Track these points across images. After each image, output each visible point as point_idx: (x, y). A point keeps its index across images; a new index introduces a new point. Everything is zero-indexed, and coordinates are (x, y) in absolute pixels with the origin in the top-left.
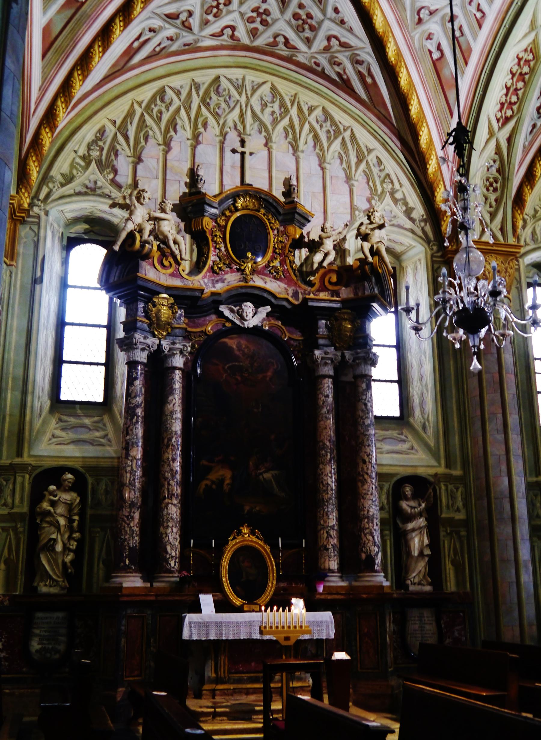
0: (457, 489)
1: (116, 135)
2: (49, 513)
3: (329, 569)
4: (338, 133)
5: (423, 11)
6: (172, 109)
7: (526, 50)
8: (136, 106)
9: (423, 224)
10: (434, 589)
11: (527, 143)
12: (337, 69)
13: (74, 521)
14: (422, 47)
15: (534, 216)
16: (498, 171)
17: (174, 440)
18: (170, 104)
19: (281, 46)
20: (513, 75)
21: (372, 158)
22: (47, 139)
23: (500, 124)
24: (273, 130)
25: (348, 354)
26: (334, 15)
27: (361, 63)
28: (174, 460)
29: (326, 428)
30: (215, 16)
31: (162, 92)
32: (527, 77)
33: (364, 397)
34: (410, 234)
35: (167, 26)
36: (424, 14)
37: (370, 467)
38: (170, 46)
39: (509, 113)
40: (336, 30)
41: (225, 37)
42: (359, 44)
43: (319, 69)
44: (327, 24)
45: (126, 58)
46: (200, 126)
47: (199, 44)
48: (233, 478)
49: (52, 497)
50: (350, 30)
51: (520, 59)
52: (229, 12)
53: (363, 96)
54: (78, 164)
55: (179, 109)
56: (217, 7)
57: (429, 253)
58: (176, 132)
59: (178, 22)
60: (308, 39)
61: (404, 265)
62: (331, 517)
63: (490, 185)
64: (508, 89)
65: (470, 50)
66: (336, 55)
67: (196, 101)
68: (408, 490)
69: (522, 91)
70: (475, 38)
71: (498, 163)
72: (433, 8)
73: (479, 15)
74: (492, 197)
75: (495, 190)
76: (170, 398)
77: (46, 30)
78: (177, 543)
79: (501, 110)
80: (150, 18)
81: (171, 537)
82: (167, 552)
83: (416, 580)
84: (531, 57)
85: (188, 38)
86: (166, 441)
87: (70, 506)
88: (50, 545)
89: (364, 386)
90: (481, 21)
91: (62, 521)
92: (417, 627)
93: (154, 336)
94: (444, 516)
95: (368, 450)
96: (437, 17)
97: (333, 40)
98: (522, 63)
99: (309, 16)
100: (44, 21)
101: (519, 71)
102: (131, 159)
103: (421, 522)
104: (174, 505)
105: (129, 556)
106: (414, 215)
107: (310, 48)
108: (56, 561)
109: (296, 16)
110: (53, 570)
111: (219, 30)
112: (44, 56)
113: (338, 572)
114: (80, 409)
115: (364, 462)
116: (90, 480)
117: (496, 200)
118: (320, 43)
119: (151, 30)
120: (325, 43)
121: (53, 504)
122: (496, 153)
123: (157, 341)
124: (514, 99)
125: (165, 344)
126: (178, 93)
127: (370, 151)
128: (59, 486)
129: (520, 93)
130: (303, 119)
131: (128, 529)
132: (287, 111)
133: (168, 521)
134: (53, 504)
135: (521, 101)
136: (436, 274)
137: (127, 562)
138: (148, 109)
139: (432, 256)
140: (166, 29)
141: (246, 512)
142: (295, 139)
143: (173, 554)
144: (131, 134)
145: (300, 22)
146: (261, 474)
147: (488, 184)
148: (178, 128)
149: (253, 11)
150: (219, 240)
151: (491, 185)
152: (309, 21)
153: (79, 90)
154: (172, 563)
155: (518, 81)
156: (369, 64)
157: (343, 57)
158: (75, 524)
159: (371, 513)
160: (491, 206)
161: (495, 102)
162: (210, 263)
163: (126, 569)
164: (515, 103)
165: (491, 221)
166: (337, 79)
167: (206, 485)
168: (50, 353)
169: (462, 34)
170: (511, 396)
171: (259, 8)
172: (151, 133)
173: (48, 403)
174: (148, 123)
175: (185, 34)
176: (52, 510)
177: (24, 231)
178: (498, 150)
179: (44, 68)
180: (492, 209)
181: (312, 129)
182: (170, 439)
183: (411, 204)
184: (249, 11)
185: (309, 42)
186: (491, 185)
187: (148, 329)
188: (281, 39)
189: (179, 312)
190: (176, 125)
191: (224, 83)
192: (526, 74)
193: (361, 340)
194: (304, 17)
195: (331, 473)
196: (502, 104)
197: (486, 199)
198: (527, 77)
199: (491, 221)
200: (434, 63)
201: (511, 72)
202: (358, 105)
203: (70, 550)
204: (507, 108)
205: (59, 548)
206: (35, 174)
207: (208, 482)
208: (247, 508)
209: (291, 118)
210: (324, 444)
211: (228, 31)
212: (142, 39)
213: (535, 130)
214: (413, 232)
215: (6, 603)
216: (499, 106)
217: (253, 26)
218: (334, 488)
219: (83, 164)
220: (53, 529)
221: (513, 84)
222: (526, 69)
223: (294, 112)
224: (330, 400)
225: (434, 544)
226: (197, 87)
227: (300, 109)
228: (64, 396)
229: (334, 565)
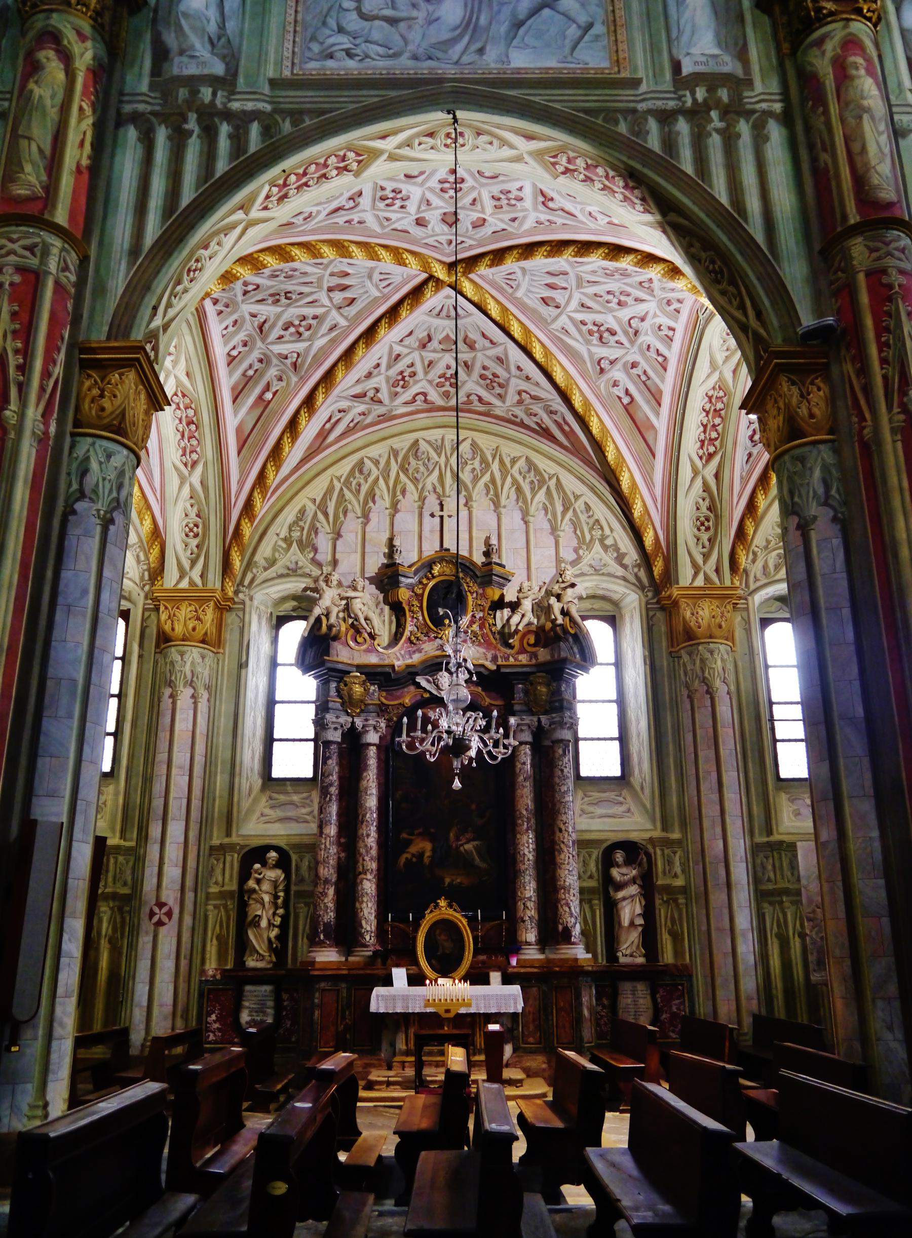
0: (675, 853)
1: (316, 512)
2: (254, 891)
3: (526, 942)
4: (542, 482)
5: (602, 361)
6: (370, 480)
7: (714, 388)
8: (336, 482)
9: (636, 570)
10: (647, 961)
11: (744, 474)
12: (535, 419)
13: (278, 897)
14: (610, 394)
15: (766, 547)
16: (709, 509)
17: (368, 815)
18: (369, 475)
19: (476, 403)
20: (707, 413)
21: (579, 505)
22: (247, 530)
23: (704, 462)
24: (474, 488)
25: (544, 719)
26: (518, 373)
27: (555, 413)
28: (368, 836)
29: (522, 797)
30: (403, 387)
31: (360, 465)
32: (723, 412)
33: (561, 763)
34: (622, 582)
35: (356, 404)
36: (604, 364)
37: (566, 835)
38: (364, 420)
39: (712, 449)
40: (524, 386)
41: (418, 403)
42: (551, 397)
43: (518, 420)
44: (513, 381)
45: (321, 439)
46: (398, 493)
47: (394, 413)
48: (434, 850)
49: (257, 876)
50: (537, 384)
51: (710, 398)
52: (416, 382)
53: (566, 443)
54: (280, 546)
55: (377, 479)
56: (403, 379)
57: (644, 600)
58: (374, 502)
59: (367, 399)
60: (499, 394)
61: (623, 612)
62: (527, 888)
63: (701, 524)
64: (705, 426)
65: (661, 392)
66: (530, 407)
67: (394, 468)
68: (619, 856)
69: (721, 426)
70: (663, 381)
71: (708, 500)
72: (612, 358)
73: (660, 359)
74: (705, 537)
75: (708, 529)
76: (365, 774)
77: (239, 430)
78: (372, 917)
79: (702, 447)
80: (336, 402)
81: (366, 911)
82: (362, 927)
83: (628, 952)
84: (721, 394)
85: (381, 410)
86: (360, 817)
87: (275, 884)
88: (256, 922)
89: (560, 751)
90: (664, 364)
91: (267, 898)
92: (629, 1001)
93: (348, 714)
94: (659, 882)
95: (564, 818)
96: (619, 366)
97: (524, 394)
98: (713, 400)
99: (495, 375)
100: (236, 422)
101: (713, 408)
102: (330, 536)
103: (633, 890)
104: (369, 880)
105: (324, 931)
106: (627, 561)
107: (504, 402)
108: (261, 936)
109: (482, 377)
110: (260, 945)
111: (411, 398)
112: (239, 453)
113: (537, 945)
114: (291, 785)
115: (561, 830)
116: (294, 857)
117: (709, 540)
118: (512, 398)
119: (340, 411)
120: (517, 397)
121: (258, 881)
122: (704, 491)
123: (350, 719)
124: (714, 435)
125: (359, 722)
126: (376, 463)
127: (577, 497)
128: (264, 864)
129: (720, 428)
130: (504, 472)
131: (322, 905)
132: (488, 466)
133: (362, 896)
134: (258, 881)
135: (722, 436)
136: (651, 623)
137: (322, 937)
138: (347, 483)
139: (647, 603)
140: (355, 407)
141: (446, 884)
142: (497, 495)
143: (369, 928)
144: (331, 511)
145: (488, 381)
146: (462, 845)
147: (699, 523)
148: (377, 498)
149: (440, 377)
150: (416, 609)
152: (496, 379)
153: (273, 479)
154: (368, 938)
155: (714, 417)
156: (562, 413)
157: (537, 408)
158: (280, 901)
159: (567, 884)
160: (703, 547)
161: (694, 441)
162: (407, 633)
163: (321, 944)
164: (716, 439)
165: (705, 562)
166: (537, 428)
167: (407, 858)
168: (260, 732)
169: (649, 378)
170: (727, 751)
171: (445, 374)
172: (350, 507)
173: (260, 782)
174: (347, 498)
175: (376, 407)
176: (257, 888)
177: (231, 619)
178: (706, 488)
179: (240, 464)
180: (705, 550)
181: (515, 482)
182: (364, 816)
183: (623, 550)
184: (436, 378)
185: (500, 396)
186: (702, 524)
187: (341, 708)
188: (474, 398)
189: (372, 688)
190: (375, 495)
191: (423, 446)
192: (721, 410)
193: (557, 704)
194: (491, 377)
195: (528, 842)
196: (702, 442)
197: (698, 540)
198: (723, 412)
199: (705, 562)
200: (626, 408)
201: (704, 410)
202: (563, 451)
203: (274, 926)
204: (708, 445)
205: (264, 923)
206: (237, 563)
207: (409, 856)
208: (447, 880)
209: (492, 474)
210: (521, 813)
211: (421, 397)
212: (333, 421)
213: (751, 459)
214: (624, 579)
215: (218, 977)
216: (699, 444)
217: (444, 389)
218: (531, 858)
219: (284, 546)
220: (259, 906)
221: (708, 420)
222: (719, 406)
223: (495, 467)
224: (528, 767)
225: (649, 913)
226: (395, 453)
227: (502, 462)
228: (275, 774)
229: (531, 936)
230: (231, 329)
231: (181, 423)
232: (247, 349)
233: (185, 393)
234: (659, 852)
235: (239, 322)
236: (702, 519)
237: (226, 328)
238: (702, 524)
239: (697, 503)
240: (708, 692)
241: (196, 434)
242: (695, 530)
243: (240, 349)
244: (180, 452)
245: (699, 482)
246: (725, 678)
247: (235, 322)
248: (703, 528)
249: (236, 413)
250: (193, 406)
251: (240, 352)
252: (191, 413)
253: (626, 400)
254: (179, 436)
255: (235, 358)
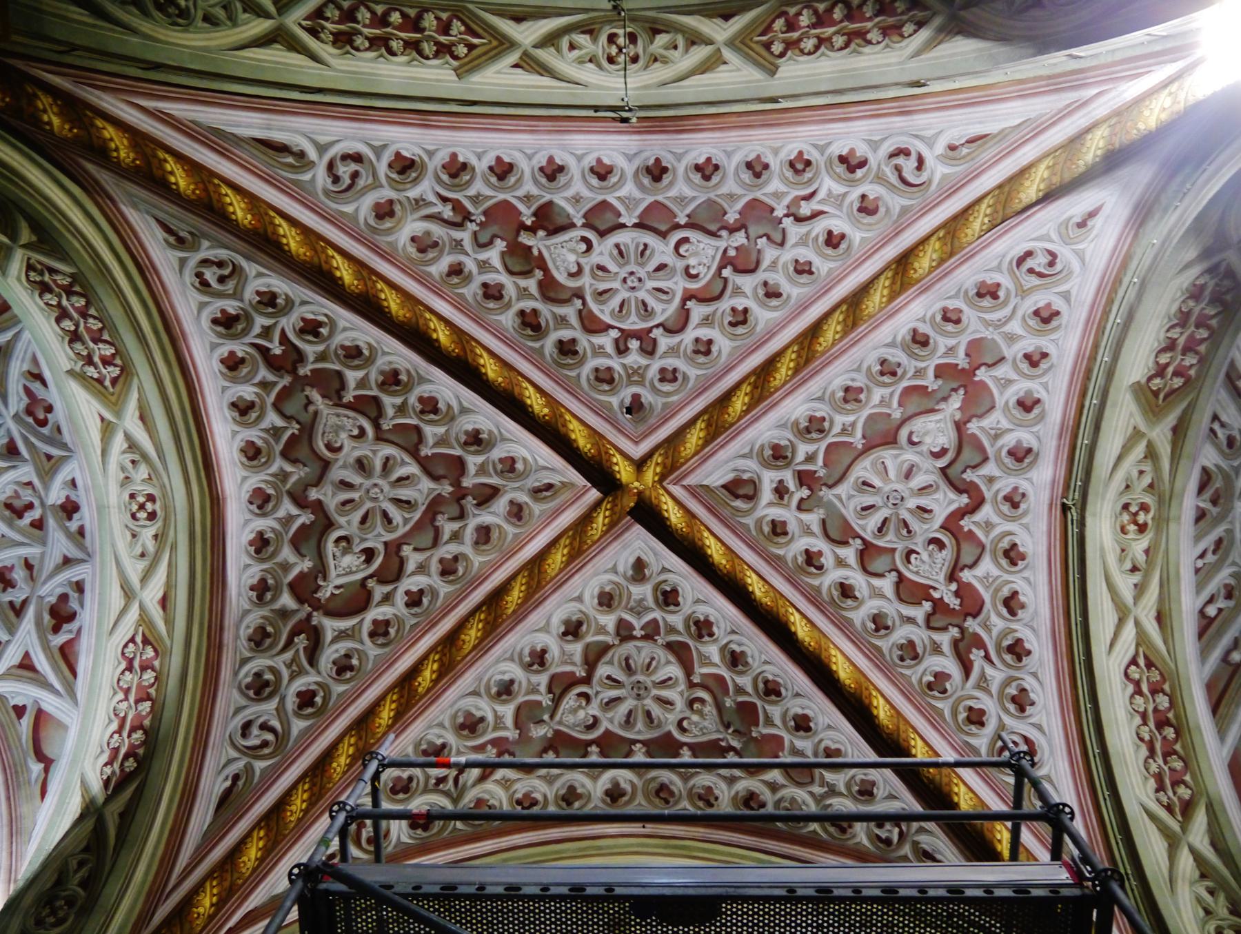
100: (1226, 751)
230: (1210, 558)
231: (1145, 723)
232: (1231, 603)
233: (1152, 658)
235: (1225, 543)
237: (1202, 556)
241: (1178, 747)
243: (1221, 604)
244: (1152, 783)
247: (1219, 542)
249: (1222, 733)
250: (1166, 687)
251: (1220, 610)
252: (1163, 701)
254: (1144, 751)
255: (1211, 620)
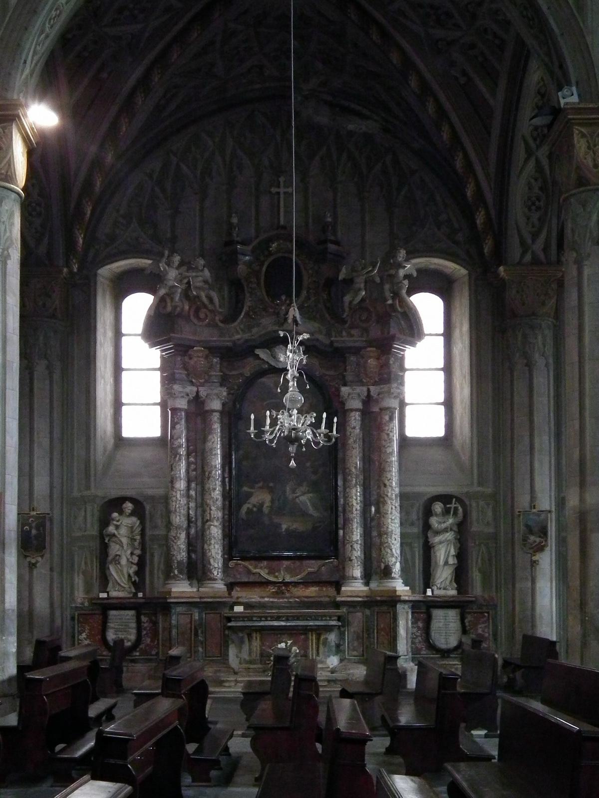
2: (114, 535)
13: (135, 540)
16: (541, 189)
25: (372, 388)
28: (215, 489)
29: (352, 457)
33: (387, 428)
37: (390, 490)
48: (272, 501)
49: (115, 522)
62: (355, 533)
74: (535, 217)
78: (219, 557)
81: (213, 552)
82: (211, 565)
87: (131, 529)
88: (117, 560)
89: (387, 418)
91: (125, 540)
95: (389, 476)
104: (216, 526)
105: (178, 568)
115: (385, 485)
116: (148, 507)
117: (539, 219)
121: (117, 527)
128: (121, 512)
131: (175, 547)
133: (210, 539)
134: (117, 527)
137: (176, 572)
141: (283, 530)
143: (216, 566)
146: (297, 497)
151: (534, 204)
154: (215, 573)
158: (136, 544)
159: (390, 530)
160: (533, 227)
163: (175, 578)
165: (533, 241)
167: (248, 508)
176: (116, 533)
193: (385, 376)
195: (356, 495)
197: (528, 219)
205: (124, 561)
207: (250, 506)
208: (284, 527)
210: (350, 471)
218: (359, 508)
220: (118, 547)
224: (357, 431)
234: (474, 504)
236: (534, 199)
238: (534, 204)
239: (529, 183)
240: (527, 365)
242: (526, 210)
245: (532, 164)
246: (545, 351)
248: (533, 208)
253: (463, 80)
